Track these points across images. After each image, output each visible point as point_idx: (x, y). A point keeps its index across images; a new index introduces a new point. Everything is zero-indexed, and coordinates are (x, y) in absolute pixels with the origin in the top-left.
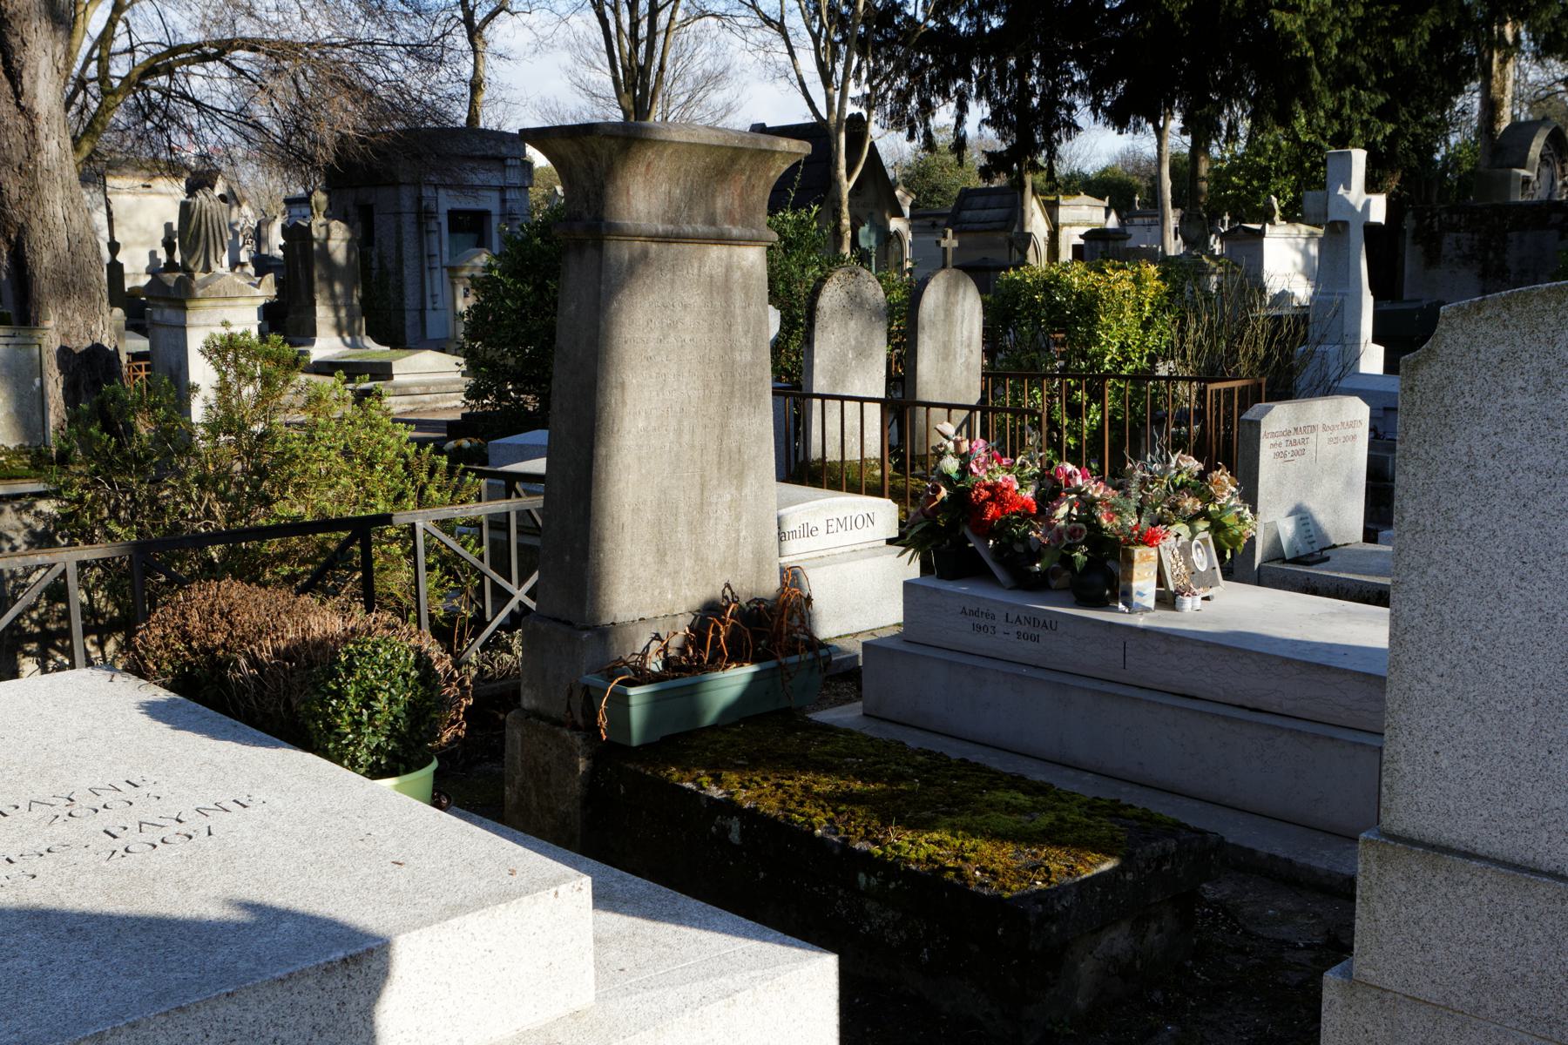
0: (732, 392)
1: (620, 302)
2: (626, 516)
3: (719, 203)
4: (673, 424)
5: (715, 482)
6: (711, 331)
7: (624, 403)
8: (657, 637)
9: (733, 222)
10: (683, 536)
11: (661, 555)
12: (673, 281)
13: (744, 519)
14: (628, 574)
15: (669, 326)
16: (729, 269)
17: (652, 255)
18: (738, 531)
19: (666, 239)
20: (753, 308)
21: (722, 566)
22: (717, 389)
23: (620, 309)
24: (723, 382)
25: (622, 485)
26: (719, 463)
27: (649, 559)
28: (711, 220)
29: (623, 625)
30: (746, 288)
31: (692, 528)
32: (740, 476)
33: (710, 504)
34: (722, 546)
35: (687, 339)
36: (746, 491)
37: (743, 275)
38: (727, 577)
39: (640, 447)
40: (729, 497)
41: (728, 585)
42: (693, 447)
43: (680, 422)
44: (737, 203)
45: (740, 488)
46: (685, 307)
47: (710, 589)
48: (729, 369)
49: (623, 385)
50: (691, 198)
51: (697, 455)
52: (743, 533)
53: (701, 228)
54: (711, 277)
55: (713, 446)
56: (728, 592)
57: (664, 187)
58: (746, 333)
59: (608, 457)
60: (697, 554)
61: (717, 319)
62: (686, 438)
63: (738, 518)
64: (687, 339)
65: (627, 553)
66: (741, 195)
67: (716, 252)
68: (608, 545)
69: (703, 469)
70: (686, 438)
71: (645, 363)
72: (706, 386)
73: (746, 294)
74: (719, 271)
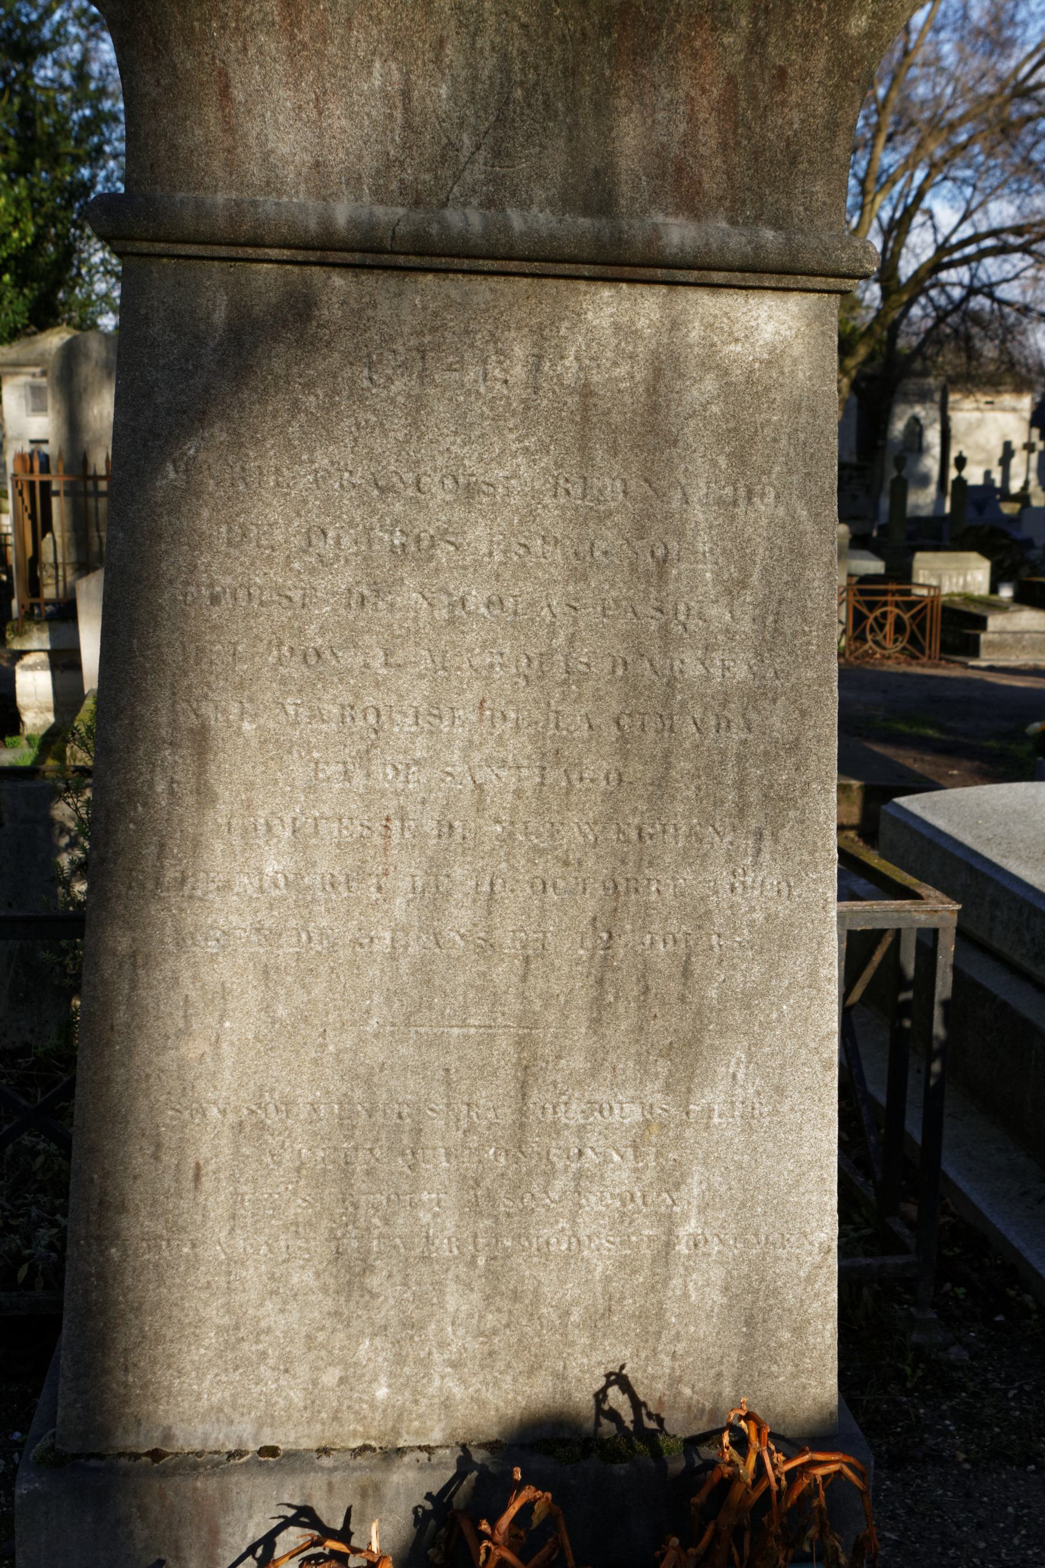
0: (662, 784)
1: (190, 467)
2: (211, 1142)
3: (630, 137)
4: (408, 873)
5: (578, 1062)
6: (579, 576)
7: (205, 795)
8: (305, 1516)
9: (691, 205)
10: (437, 1213)
11: (350, 1273)
12: (418, 404)
13: (694, 1187)
14: (214, 1313)
15: (399, 554)
16: (664, 369)
17: (331, 311)
18: (669, 1222)
19: (371, 253)
20: (765, 506)
21: (599, 1321)
22: (597, 767)
23: (193, 491)
24: (624, 745)
25: (194, 1048)
26: (598, 1003)
27: (302, 1278)
28: (596, 194)
29: (194, 1463)
30: (740, 443)
31: (475, 1197)
32: (685, 1057)
33: (556, 1129)
34: (601, 1256)
35: (476, 599)
36: (711, 1097)
37: (727, 389)
38: (617, 1352)
39: (272, 937)
40: (634, 1114)
41: (619, 1379)
42: (487, 948)
43: (436, 866)
44: (709, 137)
45: (683, 1083)
46: (470, 492)
47: (571, 1376)
48: (647, 707)
49: (201, 740)
50: (503, 115)
51: (504, 973)
52: (691, 1227)
53: (533, 219)
54: (586, 392)
55: (571, 951)
56: (616, 1397)
57: (382, 75)
58: (733, 589)
59: (138, 960)
60: (493, 1275)
61: (608, 538)
62: (461, 917)
63: (672, 1180)
64: (476, 599)
65: (214, 1252)
66: (727, 106)
67: (612, 317)
68: (139, 1224)
69: (528, 1021)
70: (461, 917)
71: (294, 670)
72: (552, 756)
73: (740, 458)
74: (622, 376)
